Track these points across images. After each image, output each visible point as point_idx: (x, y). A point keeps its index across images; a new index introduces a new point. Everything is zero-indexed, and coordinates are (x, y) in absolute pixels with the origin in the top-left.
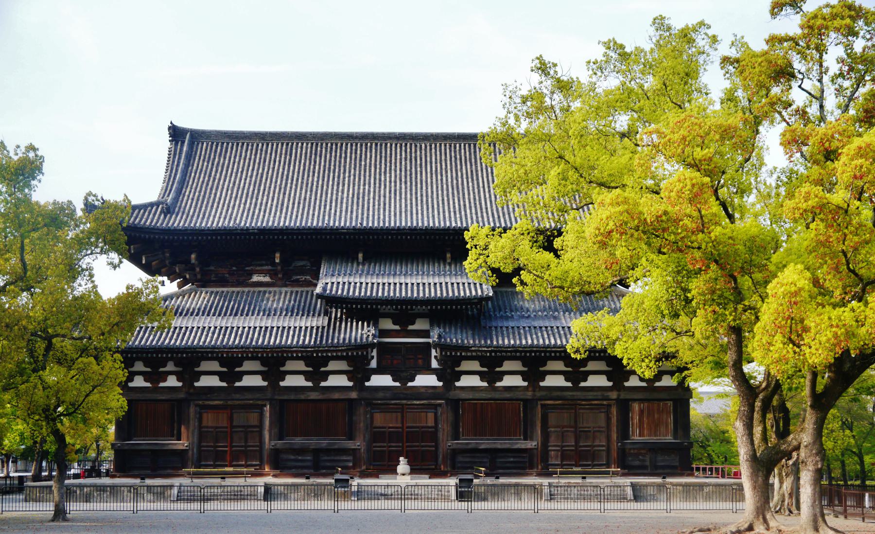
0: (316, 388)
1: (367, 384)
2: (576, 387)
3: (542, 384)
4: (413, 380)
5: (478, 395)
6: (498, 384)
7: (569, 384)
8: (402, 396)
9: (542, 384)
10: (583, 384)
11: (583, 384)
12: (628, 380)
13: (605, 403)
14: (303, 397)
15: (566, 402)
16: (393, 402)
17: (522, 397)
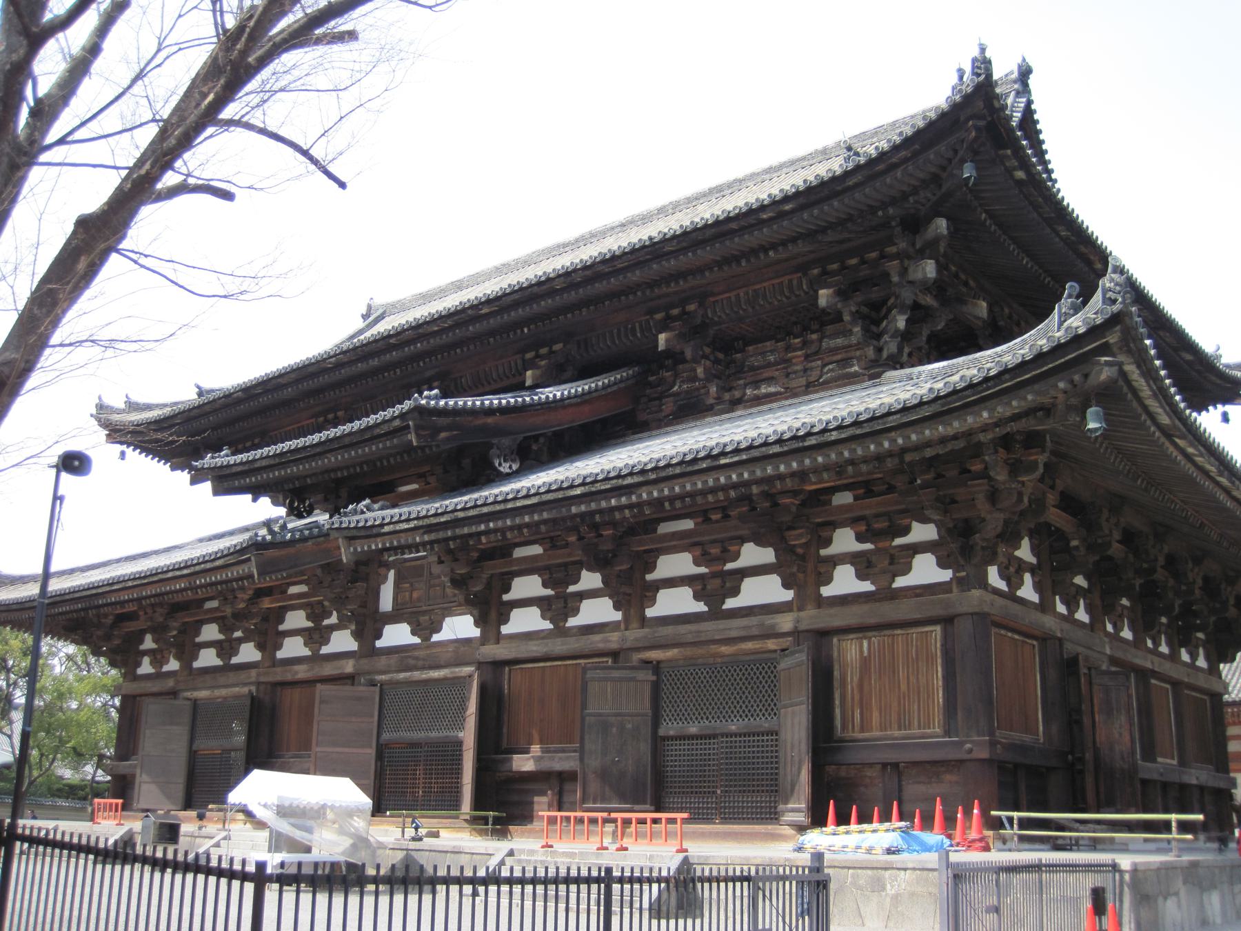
0: (316, 658)
1: (379, 644)
2: (716, 613)
3: (650, 613)
4: (438, 629)
5: (535, 649)
6: (572, 622)
7: (701, 607)
8: (412, 662)
9: (650, 613)
10: (730, 603)
11: (730, 603)
12: (829, 580)
13: (771, 644)
14: (289, 677)
15: (689, 652)
16: (402, 676)
17: (601, 646)
